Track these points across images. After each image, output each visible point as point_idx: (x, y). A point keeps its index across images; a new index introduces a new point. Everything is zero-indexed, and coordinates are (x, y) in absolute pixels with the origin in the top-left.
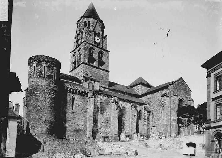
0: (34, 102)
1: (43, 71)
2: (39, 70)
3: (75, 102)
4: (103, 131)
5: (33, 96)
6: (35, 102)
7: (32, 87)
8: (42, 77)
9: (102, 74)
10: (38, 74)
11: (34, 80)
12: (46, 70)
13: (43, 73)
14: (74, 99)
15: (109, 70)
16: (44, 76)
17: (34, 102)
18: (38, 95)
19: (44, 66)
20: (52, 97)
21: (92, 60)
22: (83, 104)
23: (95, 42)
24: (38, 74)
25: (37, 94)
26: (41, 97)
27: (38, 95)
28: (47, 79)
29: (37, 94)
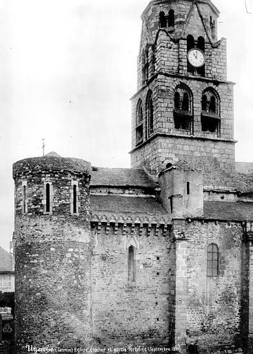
0: (28, 279)
1: (45, 197)
2: (35, 195)
3: (137, 257)
4: (218, 326)
5: (24, 263)
6: (30, 280)
7: (22, 240)
8: (42, 214)
9: (215, 156)
10: (33, 207)
11: (26, 223)
12: (52, 193)
13: (44, 202)
14: (131, 249)
15: (235, 139)
16: (48, 210)
17: (28, 279)
18: (35, 261)
19: (45, 183)
20: (70, 261)
21: (182, 121)
22: (158, 258)
23: (191, 68)
24: (33, 207)
25: (34, 258)
26: (42, 266)
27: (35, 261)
28: (55, 218)
29: (34, 258)
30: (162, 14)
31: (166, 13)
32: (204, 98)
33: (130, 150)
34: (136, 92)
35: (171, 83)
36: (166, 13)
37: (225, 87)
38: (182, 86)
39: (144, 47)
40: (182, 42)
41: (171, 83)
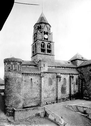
0: (7, 86)
1: (11, 67)
3: (33, 81)
4: (51, 96)
9: (50, 58)
10: (9, 69)
11: (7, 73)
12: (13, 66)
13: (11, 68)
14: (31, 79)
15: (55, 55)
16: (12, 70)
17: (7, 86)
18: (9, 82)
21: (43, 50)
23: (45, 39)
24: (9, 69)
25: (9, 81)
27: (9, 82)
28: (14, 72)
29: (9, 81)
30: (38, 26)
31: (39, 26)
32: (48, 45)
33: (31, 57)
34: (32, 44)
35: (40, 42)
36: (39, 26)
37: (52, 43)
38: (43, 42)
39: (34, 33)
40: (43, 33)
41: (40, 42)
